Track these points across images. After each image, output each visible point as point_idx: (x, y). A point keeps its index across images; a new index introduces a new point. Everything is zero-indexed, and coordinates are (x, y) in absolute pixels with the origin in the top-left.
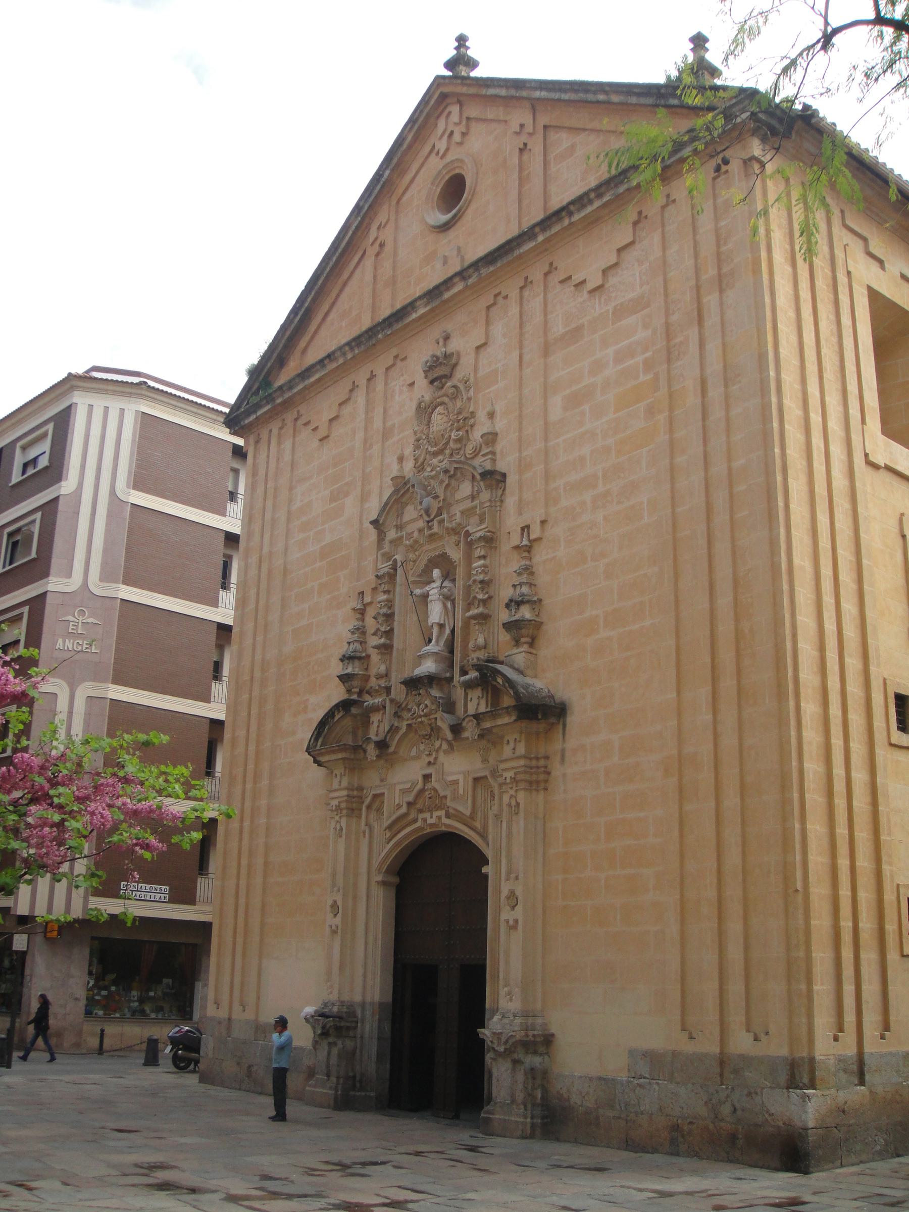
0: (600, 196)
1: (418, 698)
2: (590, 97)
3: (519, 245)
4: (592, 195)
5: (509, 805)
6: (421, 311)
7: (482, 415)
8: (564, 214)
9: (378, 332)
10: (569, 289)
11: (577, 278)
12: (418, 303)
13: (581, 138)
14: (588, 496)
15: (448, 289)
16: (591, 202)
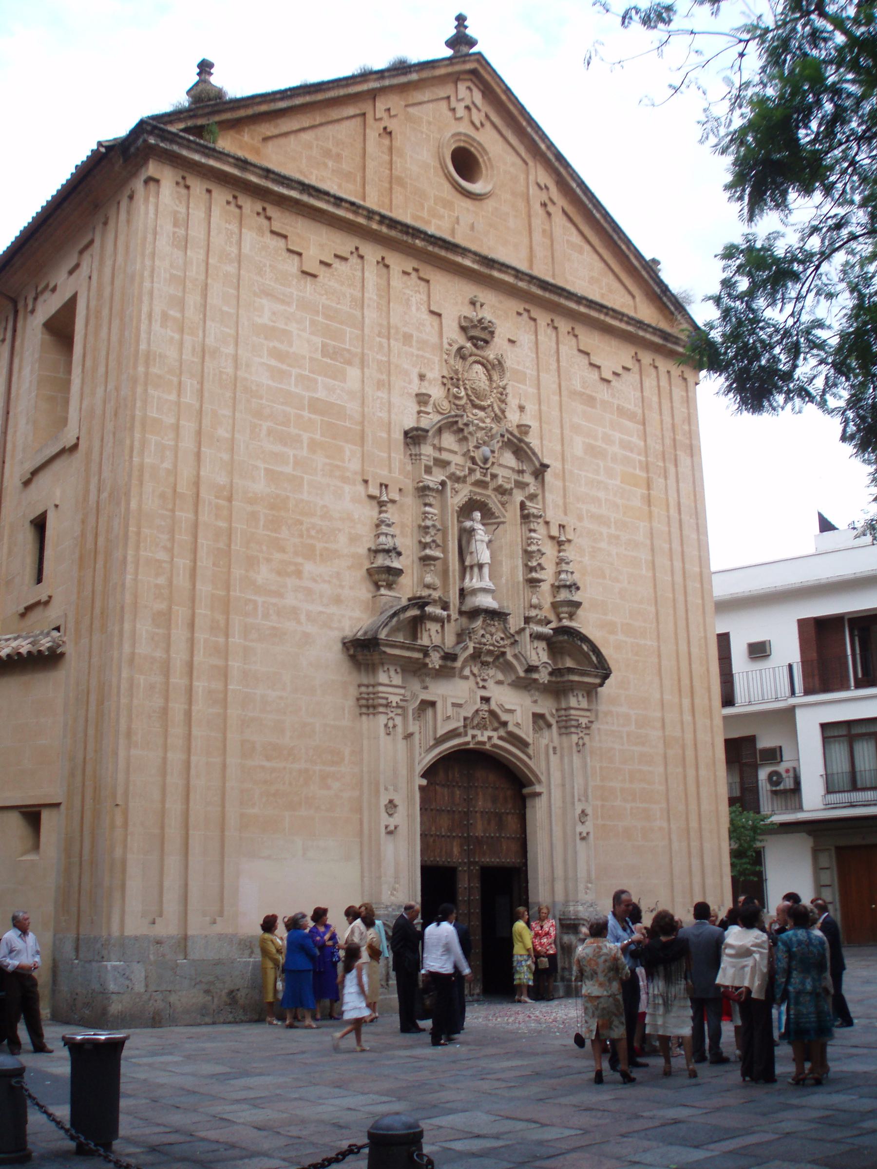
0: (628, 323)
1: (493, 630)
2: (615, 237)
3: (567, 298)
4: (625, 319)
5: (577, 744)
6: (468, 263)
7: (513, 402)
8: (605, 310)
9: (418, 237)
10: (583, 361)
11: (595, 360)
12: (470, 255)
13: (587, 248)
14: (604, 530)
15: (500, 271)
16: (621, 320)
